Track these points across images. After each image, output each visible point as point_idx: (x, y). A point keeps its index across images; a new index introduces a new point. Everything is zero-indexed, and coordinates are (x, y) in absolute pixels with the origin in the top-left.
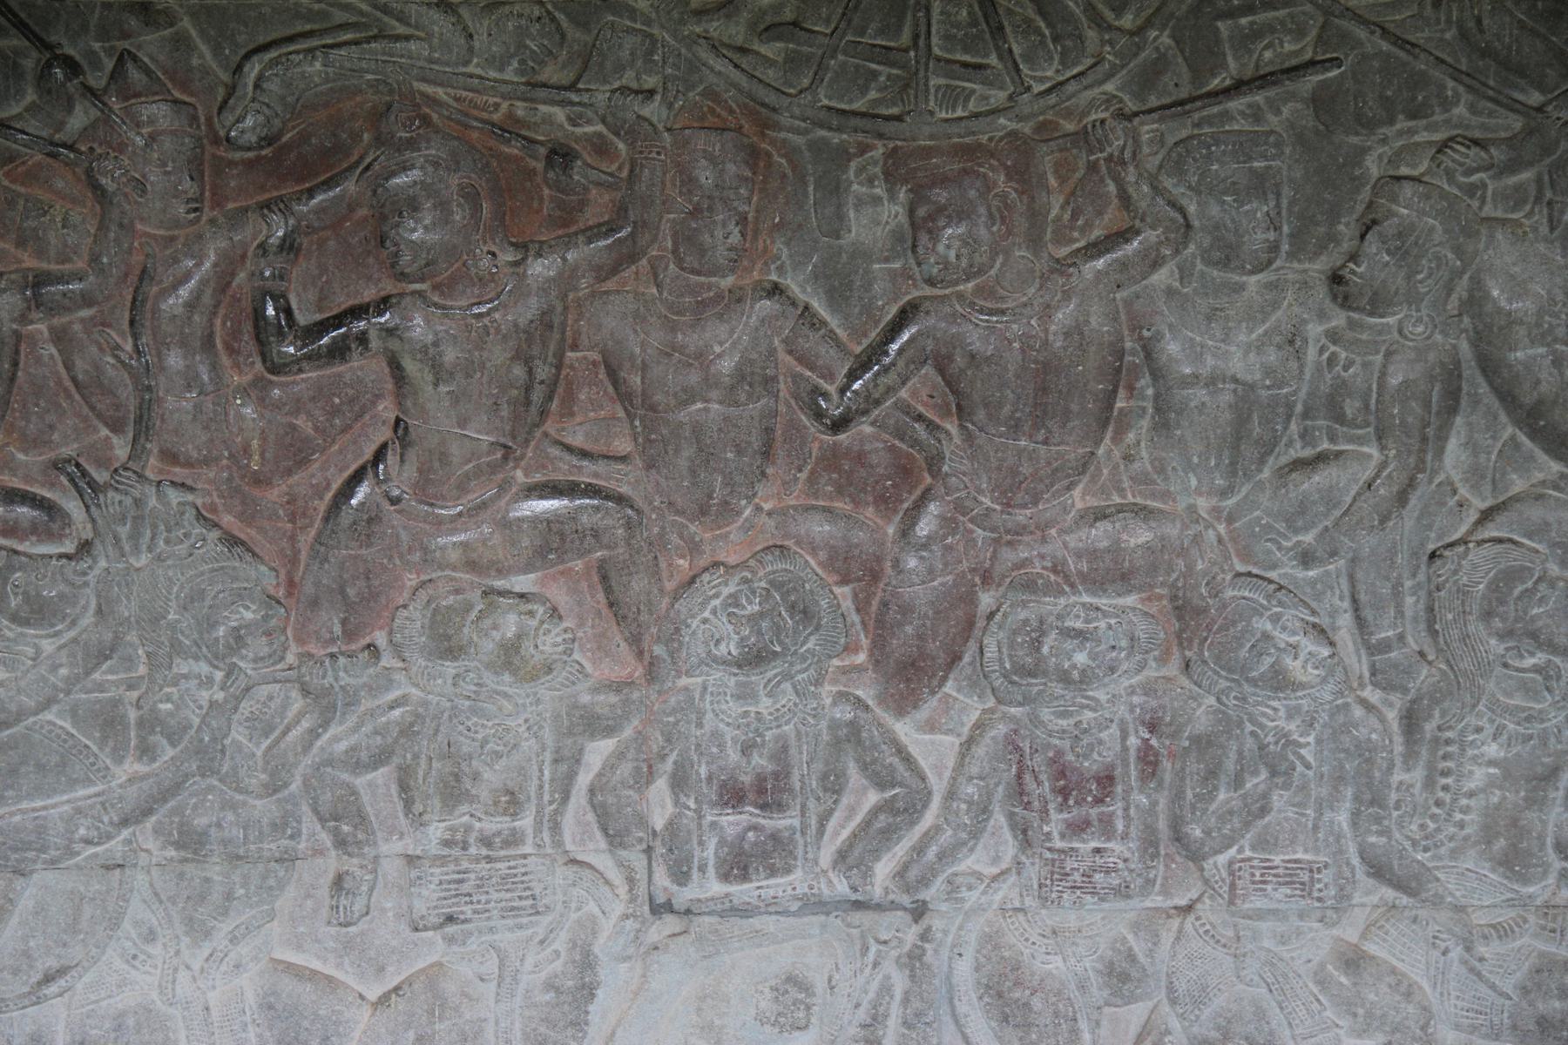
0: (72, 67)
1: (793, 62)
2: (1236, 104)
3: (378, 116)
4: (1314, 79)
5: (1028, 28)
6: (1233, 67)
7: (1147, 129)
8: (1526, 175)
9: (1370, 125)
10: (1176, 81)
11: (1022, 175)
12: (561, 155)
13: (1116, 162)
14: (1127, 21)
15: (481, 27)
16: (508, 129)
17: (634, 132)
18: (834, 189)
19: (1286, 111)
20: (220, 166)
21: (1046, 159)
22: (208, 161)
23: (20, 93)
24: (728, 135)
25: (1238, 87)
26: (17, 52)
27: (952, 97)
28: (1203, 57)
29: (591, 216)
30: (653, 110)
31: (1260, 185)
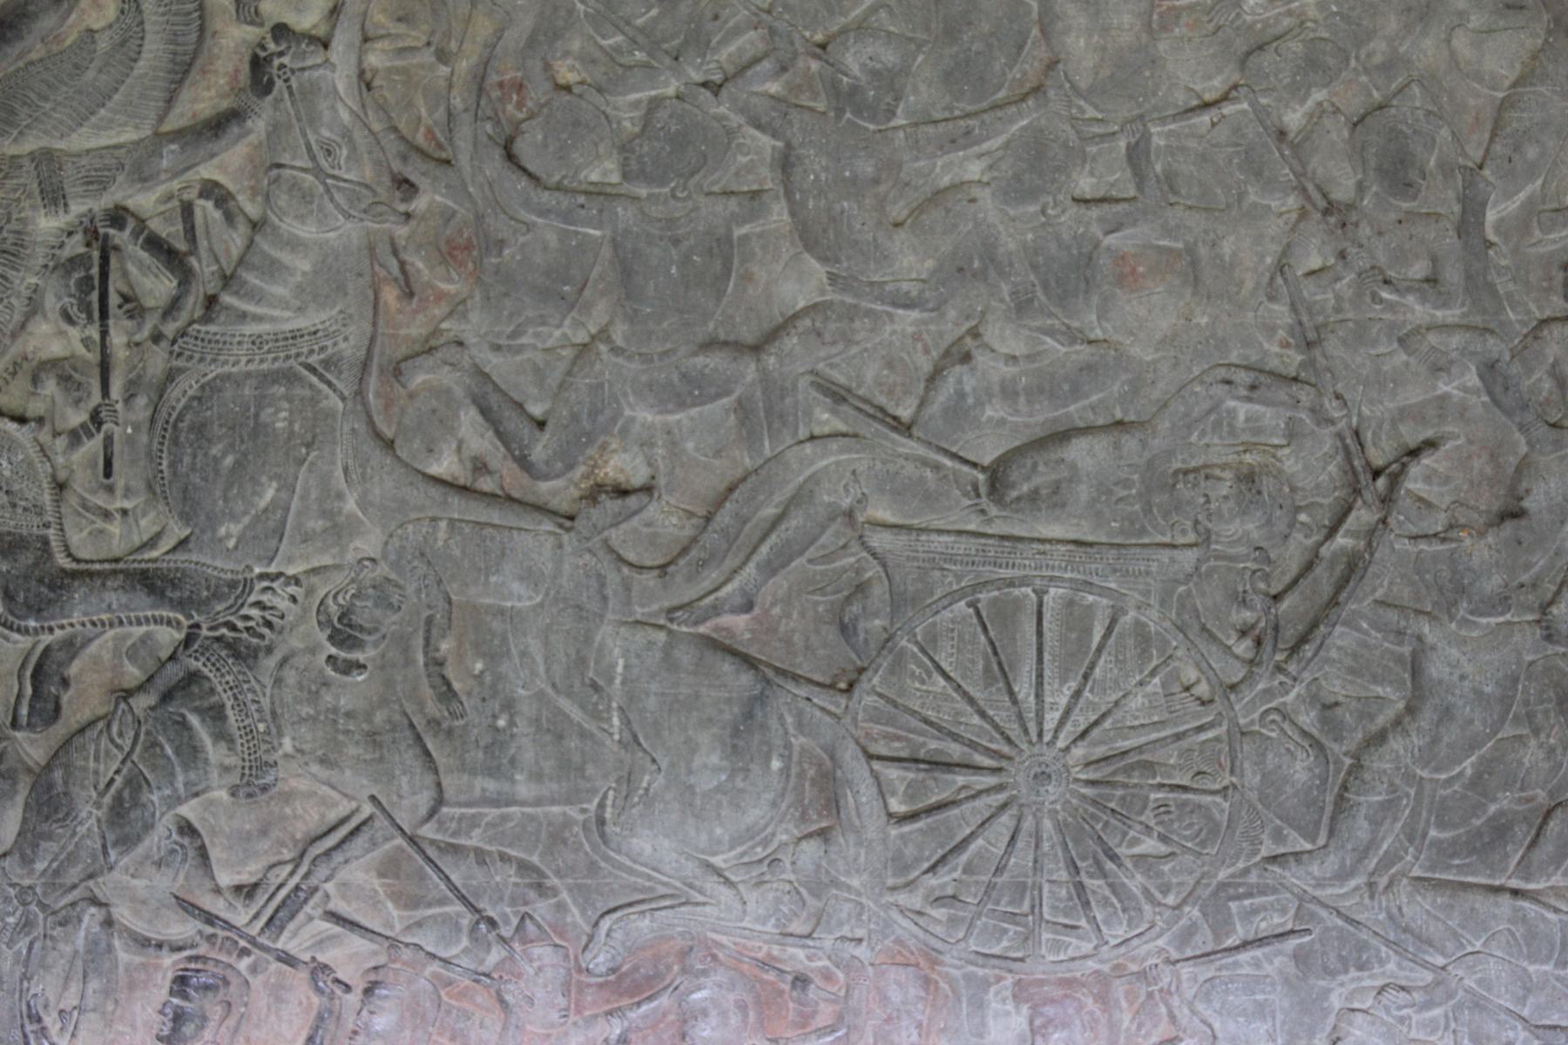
0: (492, 923)
1: (953, 922)
2: (1244, 957)
3: (684, 954)
4: (1292, 943)
5: (1106, 902)
6: (1240, 933)
7: (1186, 970)
8: (1437, 1012)
9: (1332, 974)
10: (1204, 940)
11: (1103, 998)
12: (801, 981)
13: (1166, 993)
14: (1171, 900)
15: (752, 897)
16: (766, 964)
17: (850, 966)
18: (979, 1005)
19: (1276, 961)
20: (581, 988)
21: (1119, 989)
22: (574, 984)
23: (459, 941)
24: (910, 969)
25: (1245, 945)
26: (458, 915)
27: (1057, 946)
28: (1221, 926)
29: (821, 1021)
30: (862, 952)
31: (1261, 1011)
